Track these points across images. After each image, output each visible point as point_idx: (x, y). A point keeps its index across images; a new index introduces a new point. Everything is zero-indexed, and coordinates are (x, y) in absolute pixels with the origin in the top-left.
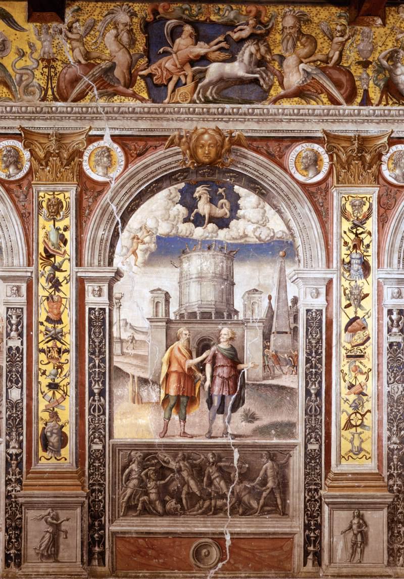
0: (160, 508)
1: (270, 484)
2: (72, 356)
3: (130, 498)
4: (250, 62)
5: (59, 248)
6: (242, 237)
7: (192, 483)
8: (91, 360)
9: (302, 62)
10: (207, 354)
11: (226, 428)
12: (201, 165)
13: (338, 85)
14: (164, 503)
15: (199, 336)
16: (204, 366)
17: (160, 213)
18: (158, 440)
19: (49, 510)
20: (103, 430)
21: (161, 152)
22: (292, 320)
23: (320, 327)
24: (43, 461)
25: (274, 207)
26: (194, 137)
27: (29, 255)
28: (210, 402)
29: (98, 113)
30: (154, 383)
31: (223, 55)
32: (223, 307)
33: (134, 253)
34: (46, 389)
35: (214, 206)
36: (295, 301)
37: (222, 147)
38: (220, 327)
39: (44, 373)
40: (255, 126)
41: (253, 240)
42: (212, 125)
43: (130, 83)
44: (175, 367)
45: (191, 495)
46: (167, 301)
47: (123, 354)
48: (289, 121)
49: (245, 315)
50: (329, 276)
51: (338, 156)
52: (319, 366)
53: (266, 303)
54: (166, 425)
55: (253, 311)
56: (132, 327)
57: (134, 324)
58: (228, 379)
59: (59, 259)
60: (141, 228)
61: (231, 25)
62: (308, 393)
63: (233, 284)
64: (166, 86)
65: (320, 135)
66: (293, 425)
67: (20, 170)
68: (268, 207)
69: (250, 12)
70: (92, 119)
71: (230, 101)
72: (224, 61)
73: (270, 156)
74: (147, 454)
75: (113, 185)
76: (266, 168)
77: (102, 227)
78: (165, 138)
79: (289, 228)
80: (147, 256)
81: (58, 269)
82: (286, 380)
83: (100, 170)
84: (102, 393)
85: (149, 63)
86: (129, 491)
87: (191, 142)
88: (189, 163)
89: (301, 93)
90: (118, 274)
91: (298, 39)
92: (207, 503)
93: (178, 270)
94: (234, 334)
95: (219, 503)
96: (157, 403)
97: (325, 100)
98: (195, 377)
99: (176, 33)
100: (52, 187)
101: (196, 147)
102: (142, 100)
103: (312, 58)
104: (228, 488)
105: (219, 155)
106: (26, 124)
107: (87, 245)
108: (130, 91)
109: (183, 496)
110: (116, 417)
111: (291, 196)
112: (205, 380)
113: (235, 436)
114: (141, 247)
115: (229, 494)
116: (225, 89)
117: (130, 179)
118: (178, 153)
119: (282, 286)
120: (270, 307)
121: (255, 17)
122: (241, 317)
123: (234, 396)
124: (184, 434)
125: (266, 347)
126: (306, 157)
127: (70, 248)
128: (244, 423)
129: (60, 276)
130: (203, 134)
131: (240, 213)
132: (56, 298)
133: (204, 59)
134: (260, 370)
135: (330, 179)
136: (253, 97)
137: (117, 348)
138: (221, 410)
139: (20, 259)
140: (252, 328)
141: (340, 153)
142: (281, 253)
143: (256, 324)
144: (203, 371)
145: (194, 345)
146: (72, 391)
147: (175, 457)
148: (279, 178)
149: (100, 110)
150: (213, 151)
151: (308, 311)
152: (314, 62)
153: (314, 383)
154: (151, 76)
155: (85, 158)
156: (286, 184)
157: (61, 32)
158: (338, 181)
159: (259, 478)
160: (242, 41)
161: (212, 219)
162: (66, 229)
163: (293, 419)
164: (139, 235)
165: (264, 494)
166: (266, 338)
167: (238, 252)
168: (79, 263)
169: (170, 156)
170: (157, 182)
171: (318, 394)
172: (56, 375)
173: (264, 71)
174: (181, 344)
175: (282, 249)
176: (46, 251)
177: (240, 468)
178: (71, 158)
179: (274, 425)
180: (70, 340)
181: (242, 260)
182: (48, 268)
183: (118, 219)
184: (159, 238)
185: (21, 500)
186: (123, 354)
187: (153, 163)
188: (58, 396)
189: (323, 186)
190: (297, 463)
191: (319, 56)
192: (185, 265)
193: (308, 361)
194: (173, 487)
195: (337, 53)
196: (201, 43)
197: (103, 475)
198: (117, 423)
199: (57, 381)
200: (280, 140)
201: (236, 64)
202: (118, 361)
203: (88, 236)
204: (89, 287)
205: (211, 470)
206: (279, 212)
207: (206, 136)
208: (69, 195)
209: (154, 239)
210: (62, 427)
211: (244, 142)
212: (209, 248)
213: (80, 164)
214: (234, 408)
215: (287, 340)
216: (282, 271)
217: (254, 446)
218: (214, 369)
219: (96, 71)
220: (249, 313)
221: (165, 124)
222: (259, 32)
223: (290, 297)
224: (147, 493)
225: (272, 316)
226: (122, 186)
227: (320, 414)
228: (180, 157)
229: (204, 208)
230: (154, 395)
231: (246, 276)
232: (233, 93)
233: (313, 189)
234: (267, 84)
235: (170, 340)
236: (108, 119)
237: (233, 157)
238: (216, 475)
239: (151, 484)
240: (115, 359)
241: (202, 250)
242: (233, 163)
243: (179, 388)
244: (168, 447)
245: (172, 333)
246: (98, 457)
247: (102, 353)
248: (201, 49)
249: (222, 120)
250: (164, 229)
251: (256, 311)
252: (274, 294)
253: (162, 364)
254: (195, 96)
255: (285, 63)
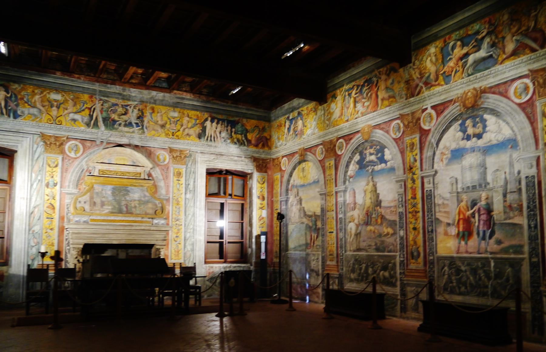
0: (458, 291)
1: (511, 282)
2: (420, 214)
3: (445, 284)
4: (488, 48)
5: (414, 164)
6: (489, 142)
7: (471, 278)
8: (428, 215)
9: (514, 36)
10: (476, 208)
11: (486, 248)
12: (468, 109)
13: (535, 40)
14: (460, 288)
15: (471, 199)
16: (475, 214)
17: (452, 138)
18: (455, 255)
19: (414, 288)
20: (433, 251)
21: (451, 108)
22: (518, 184)
23: (534, 185)
24: (412, 264)
25: (504, 121)
26: (464, 96)
27: (404, 169)
28: (478, 234)
29: (425, 98)
30: (453, 225)
31: (475, 49)
32: (482, 181)
33: (442, 160)
34: (412, 230)
35: (475, 129)
36: (519, 173)
37: (477, 96)
38: (481, 193)
39: (411, 223)
40: (491, 80)
41: (495, 142)
42: (472, 87)
43: (437, 79)
44: (461, 217)
45: (471, 284)
46: (457, 182)
47: (440, 211)
48: (509, 71)
49: (493, 184)
50: (538, 154)
51: (538, 82)
52: (535, 210)
53: (503, 176)
54: (459, 247)
55: (497, 181)
56: (443, 198)
57: (444, 196)
58: (487, 221)
59: (414, 169)
60: (444, 148)
61: (478, 33)
62: (529, 226)
63: (486, 168)
64: (451, 75)
65: (527, 73)
66: (522, 246)
67: (400, 132)
68: (501, 122)
69: (486, 21)
70: (423, 101)
71: (480, 71)
72: (476, 52)
73: (500, 94)
74: (451, 261)
75: (432, 130)
76: (499, 101)
77: (429, 150)
78: (451, 101)
79: (513, 131)
80: (447, 161)
81: (414, 174)
82: (517, 220)
83: (427, 124)
84: (432, 231)
85: (444, 66)
86: (444, 281)
87: (462, 100)
88: (462, 109)
89: (515, 54)
90: (436, 172)
91: (511, 24)
92: (479, 290)
93: (460, 165)
94: (488, 195)
95: (485, 290)
96: (455, 235)
97: (528, 52)
98: (471, 221)
99: (453, 48)
100: (410, 137)
101: (465, 101)
102: (442, 85)
103: (520, 31)
104: (489, 282)
105: (476, 101)
106: (401, 112)
107: (424, 161)
108: (437, 83)
109: (468, 285)
110: (438, 242)
111: (513, 113)
112: (475, 222)
113: (491, 253)
114: (445, 157)
115: (490, 286)
116: (477, 66)
117: (439, 125)
118: (457, 106)
119: (511, 165)
120: (506, 178)
121: (489, 23)
122: (491, 186)
123: (490, 231)
124: (467, 252)
125: (505, 201)
126: (520, 88)
127: (418, 164)
128: (495, 246)
129: (415, 177)
130: (468, 93)
131: (487, 129)
132: (414, 188)
133: (467, 55)
134: (502, 214)
135: (534, 97)
136: (490, 65)
137: (437, 208)
138: (484, 238)
139: (402, 171)
140: (496, 191)
141: (539, 79)
142: (510, 146)
143: (499, 189)
144: (474, 217)
145: (469, 204)
146: (421, 231)
147: (463, 264)
148: (506, 104)
149: (426, 96)
150: (473, 99)
151: (527, 177)
152: (521, 32)
153: (533, 220)
154: (444, 72)
155: (422, 120)
156: (509, 106)
157: (411, 67)
158: (539, 96)
159: (505, 278)
160: (483, 38)
161: (475, 135)
162: (416, 155)
163: (522, 243)
164: (444, 151)
165: (508, 287)
166: (505, 196)
167: (487, 150)
168: (422, 170)
169: (454, 108)
170: (449, 123)
171: (536, 227)
172: (415, 223)
173: (495, 49)
174: (463, 204)
175: (511, 143)
176: (410, 166)
177: (495, 271)
178: (417, 122)
179: (511, 247)
180: (420, 206)
181: (490, 154)
182: (411, 174)
183: (435, 145)
184: (452, 151)
185: (405, 282)
186: (440, 211)
187: (448, 114)
188: (416, 233)
189: (530, 102)
190: (526, 269)
191: (524, 28)
192: (464, 162)
193: (528, 207)
194: (464, 279)
195: (533, 23)
196: (465, 48)
197: (434, 272)
198: (438, 246)
199: (416, 226)
200: (505, 83)
201: (481, 51)
202: (438, 215)
203: (424, 156)
204: (426, 180)
205: (480, 271)
206: (507, 123)
207: (469, 94)
208: (416, 138)
209: (450, 152)
210: (418, 248)
211: (488, 91)
212: (474, 151)
213: (420, 124)
214: (490, 237)
215: (515, 196)
216: (511, 156)
217: (501, 259)
218: (479, 216)
219: (424, 79)
220: (495, 183)
221: (452, 94)
222: (491, 30)
223: (516, 172)
224: (452, 282)
225: (507, 183)
226: (436, 129)
227: (538, 239)
228: (459, 108)
229: (470, 131)
230: (453, 231)
231: (492, 161)
232: (481, 66)
233: (523, 106)
234: (496, 55)
235: (459, 201)
236: (429, 99)
237: (482, 100)
238: (482, 275)
239: (453, 278)
240: (437, 214)
241: (471, 152)
242: (482, 103)
243: (464, 228)
244: (460, 258)
245: (459, 198)
246: (432, 263)
247: (432, 211)
248: (465, 50)
249: (476, 83)
250: (454, 146)
251: (499, 181)
252: (507, 171)
253: (455, 215)
254: (464, 75)
255: (506, 40)
